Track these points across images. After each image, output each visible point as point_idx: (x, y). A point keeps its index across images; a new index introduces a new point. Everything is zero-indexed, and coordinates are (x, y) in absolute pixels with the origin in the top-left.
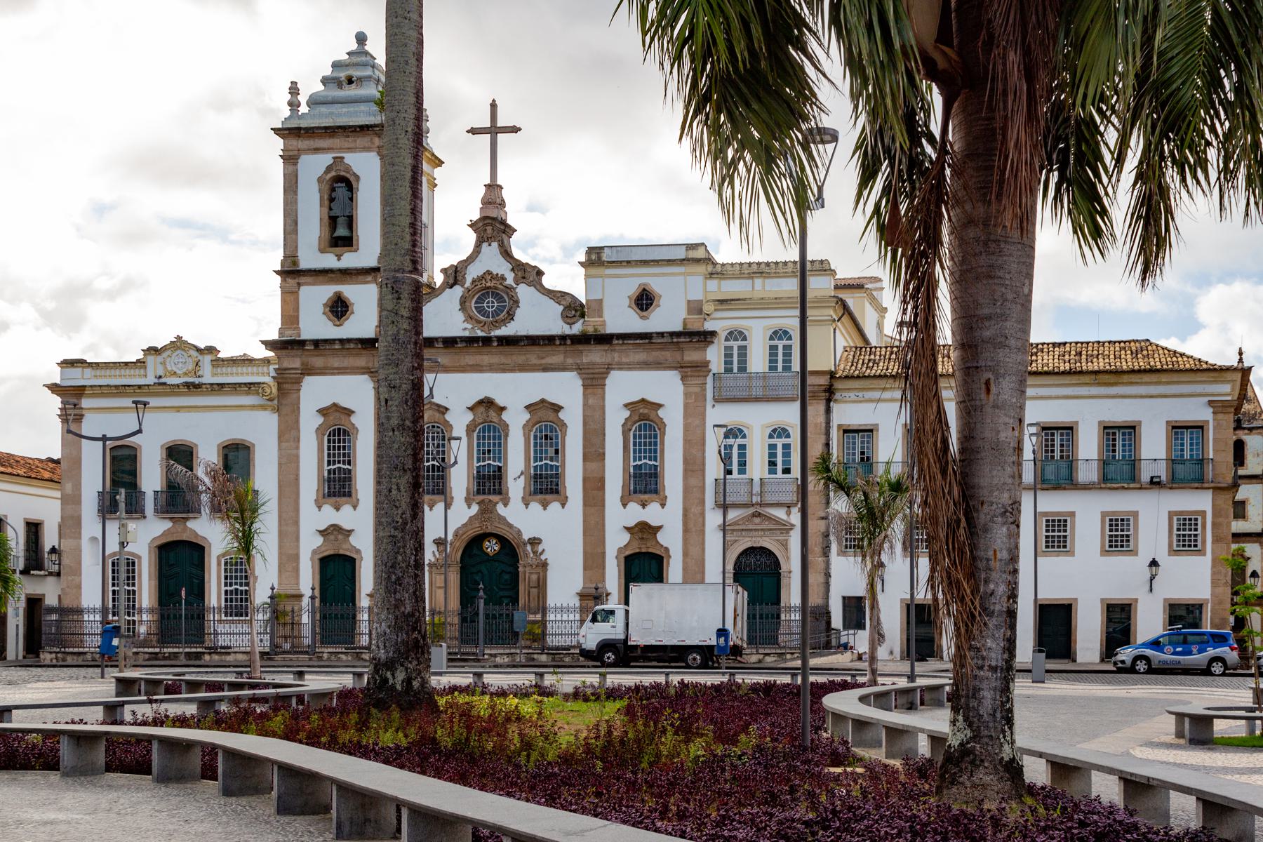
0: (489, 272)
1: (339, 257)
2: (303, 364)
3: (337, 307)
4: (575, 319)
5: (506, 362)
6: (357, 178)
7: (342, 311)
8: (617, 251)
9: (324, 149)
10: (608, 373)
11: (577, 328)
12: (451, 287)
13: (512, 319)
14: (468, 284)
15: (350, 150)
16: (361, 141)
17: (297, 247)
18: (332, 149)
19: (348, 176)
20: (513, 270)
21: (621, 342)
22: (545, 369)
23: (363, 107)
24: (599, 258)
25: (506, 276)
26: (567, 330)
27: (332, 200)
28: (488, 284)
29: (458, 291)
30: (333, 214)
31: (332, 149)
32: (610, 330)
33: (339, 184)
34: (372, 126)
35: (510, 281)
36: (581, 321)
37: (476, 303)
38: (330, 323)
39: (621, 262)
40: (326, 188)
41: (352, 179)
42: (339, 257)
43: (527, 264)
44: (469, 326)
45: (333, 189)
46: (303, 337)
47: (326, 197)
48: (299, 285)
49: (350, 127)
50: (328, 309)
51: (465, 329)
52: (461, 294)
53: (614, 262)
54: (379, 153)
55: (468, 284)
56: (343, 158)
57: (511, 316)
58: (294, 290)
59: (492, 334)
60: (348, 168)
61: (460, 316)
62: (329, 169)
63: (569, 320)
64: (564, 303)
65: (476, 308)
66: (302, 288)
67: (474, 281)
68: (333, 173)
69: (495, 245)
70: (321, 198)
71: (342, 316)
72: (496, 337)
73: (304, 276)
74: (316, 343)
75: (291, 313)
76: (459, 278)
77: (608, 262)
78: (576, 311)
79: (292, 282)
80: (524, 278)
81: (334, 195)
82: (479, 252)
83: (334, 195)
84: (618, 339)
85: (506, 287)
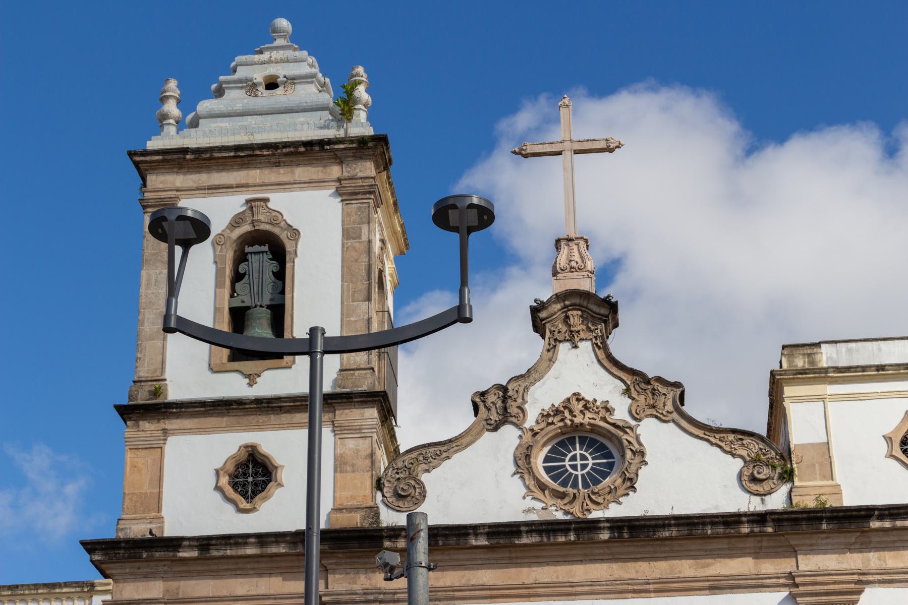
0: (578, 397)
1: (252, 378)
2: (167, 591)
3: (245, 474)
4: (766, 486)
5: (627, 576)
6: (295, 234)
7: (256, 484)
8: (849, 351)
9: (230, 187)
10: (860, 592)
11: (777, 501)
12: (496, 429)
13: (633, 488)
14: (530, 421)
15: (281, 186)
16: (302, 172)
17: (163, 362)
18: (246, 186)
19: (276, 230)
20: (627, 392)
21: (887, 524)
22: (717, 586)
23: (301, 118)
24: (812, 362)
25: (612, 404)
26: (755, 505)
27: (237, 277)
28: (578, 420)
29: (509, 436)
30: (237, 303)
31: (246, 186)
32: (850, 500)
33: (257, 248)
34: (330, 142)
35: (621, 411)
36: (784, 489)
37: (547, 459)
38: (230, 508)
39: (864, 368)
40: (230, 255)
41: (283, 236)
42: (252, 378)
43: (659, 380)
44: (539, 505)
45: (241, 257)
46: (170, 531)
47: (228, 271)
48: (165, 431)
49: (286, 145)
50: (224, 480)
51: (529, 511)
52: (517, 442)
53: (848, 369)
54: (339, 193)
55: (530, 421)
56: (266, 200)
57: (630, 483)
58: (155, 443)
59: (596, 514)
60: (276, 217)
61: (516, 487)
62: (237, 221)
63: (754, 487)
64: (744, 453)
65: (548, 470)
66: (171, 440)
67: (545, 416)
68: (246, 228)
69: (586, 347)
70: (219, 273)
71: (255, 494)
72: (608, 520)
73: (178, 416)
74: (205, 543)
75: (146, 489)
76: (513, 410)
77: (838, 369)
78: (774, 467)
79: (149, 427)
80: (653, 407)
81: (242, 268)
82: (552, 361)
83: (242, 268)
84: (881, 518)
85: (614, 425)
